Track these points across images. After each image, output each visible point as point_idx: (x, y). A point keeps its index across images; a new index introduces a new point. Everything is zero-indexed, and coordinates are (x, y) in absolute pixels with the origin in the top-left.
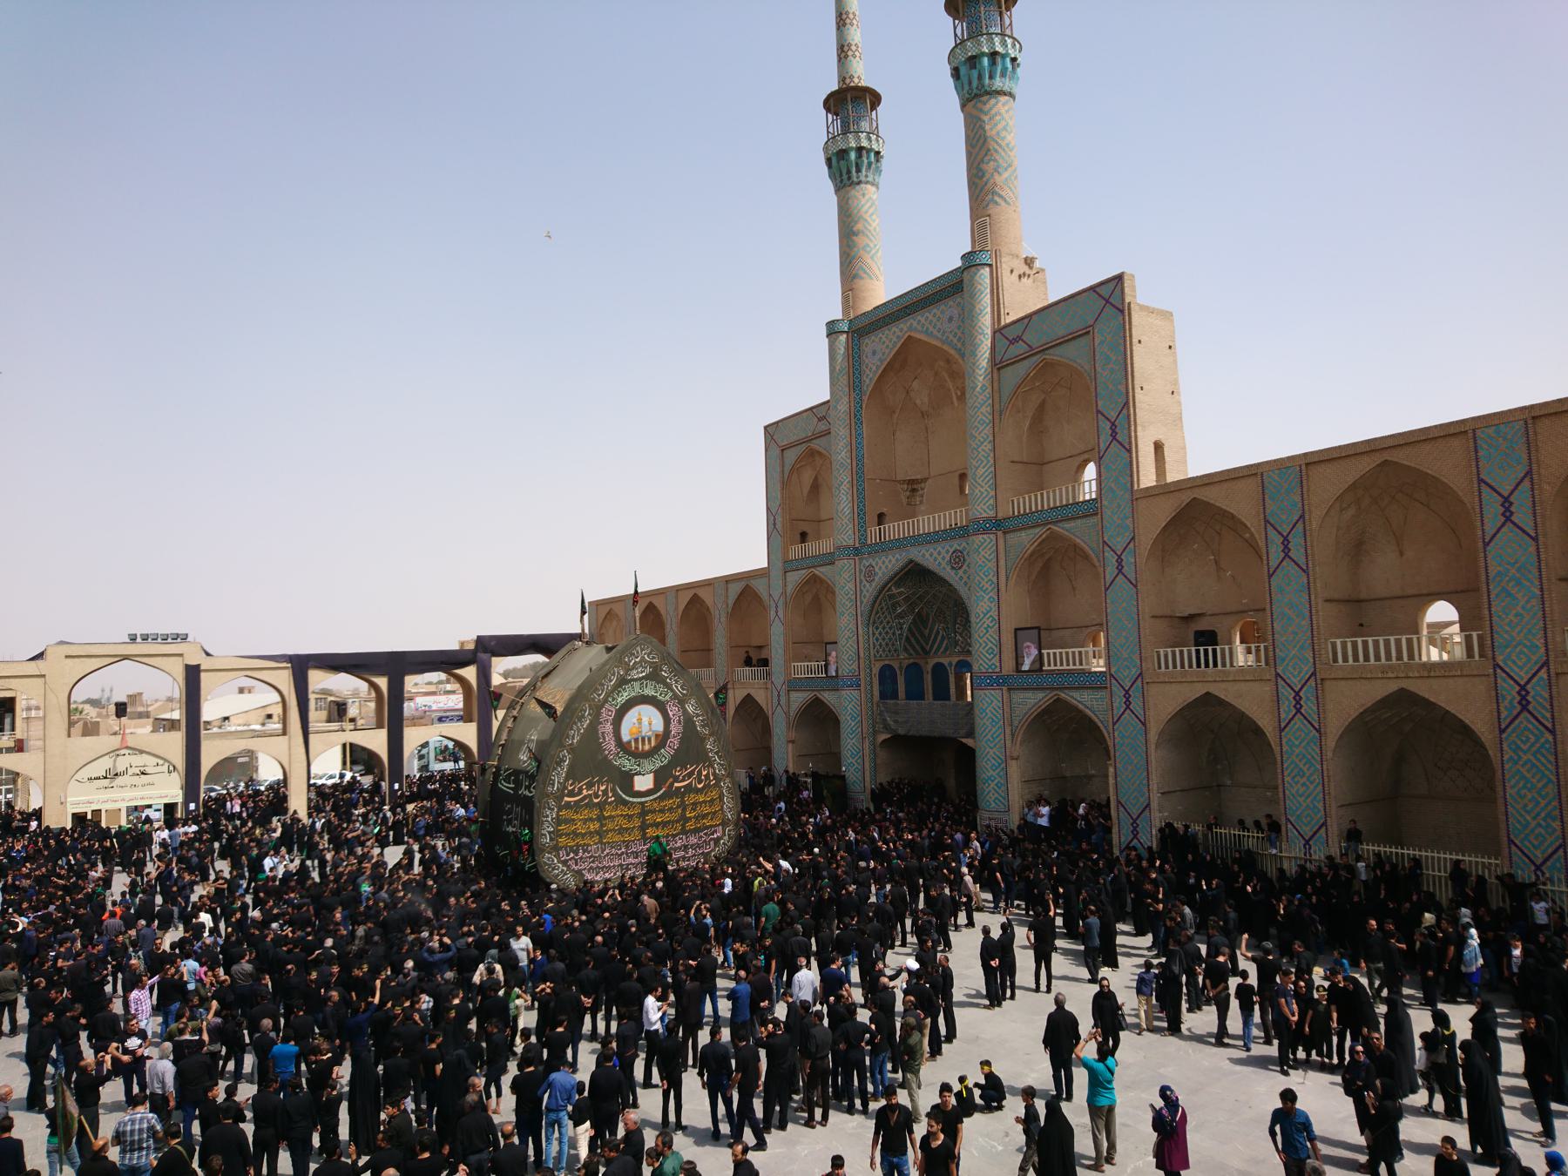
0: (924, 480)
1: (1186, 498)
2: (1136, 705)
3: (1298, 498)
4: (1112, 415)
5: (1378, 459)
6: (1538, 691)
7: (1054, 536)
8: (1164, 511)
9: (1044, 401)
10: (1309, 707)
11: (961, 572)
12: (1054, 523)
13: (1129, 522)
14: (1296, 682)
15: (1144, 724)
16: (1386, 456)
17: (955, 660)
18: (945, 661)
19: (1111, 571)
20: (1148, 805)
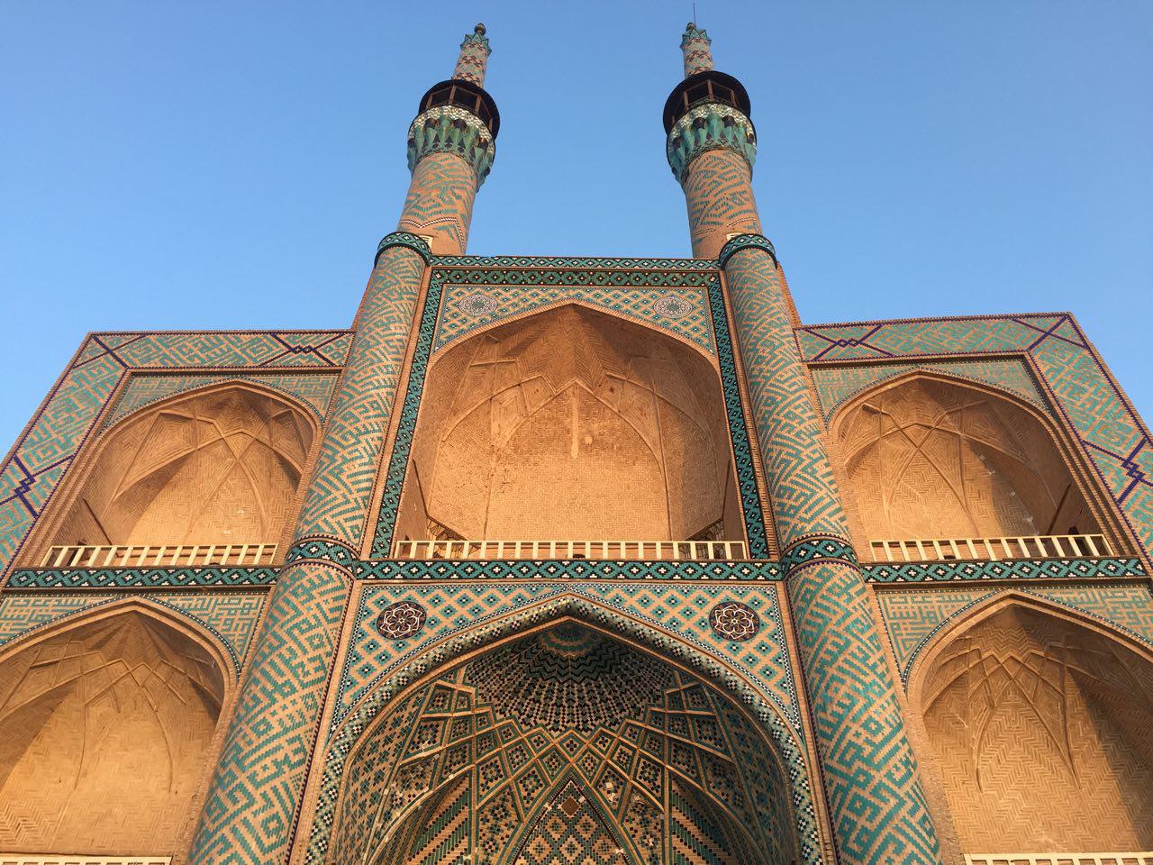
9: (876, 442)
11: (749, 648)
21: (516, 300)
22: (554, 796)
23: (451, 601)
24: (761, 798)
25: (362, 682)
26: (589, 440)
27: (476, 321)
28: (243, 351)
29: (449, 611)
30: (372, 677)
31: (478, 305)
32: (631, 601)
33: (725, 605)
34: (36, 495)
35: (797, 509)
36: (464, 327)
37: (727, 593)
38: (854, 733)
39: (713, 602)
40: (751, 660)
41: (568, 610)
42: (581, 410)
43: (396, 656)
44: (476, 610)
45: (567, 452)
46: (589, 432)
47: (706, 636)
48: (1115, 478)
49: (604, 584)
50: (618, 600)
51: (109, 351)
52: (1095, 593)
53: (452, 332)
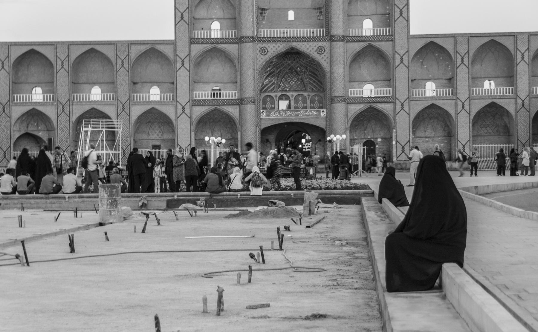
0: (267, 9)
1: (429, 40)
2: (406, 108)
3: (467, 46)
4: (401, 7)
5: (490, 38)
6: (526, 102)
7: (370, 46)
8: (420, 44)
10: (467, 107)
11: (323, 56)
12: (371, 41)
13: (406, 45)
14: (463, 100)
15: (409, 114)
16: (492, 38)
17: (279, 94)
18: (273, 95)
19: (398, 61)
20: (409, 141)
22: (289, 70)
23: (272, 47)
29: (272, 49)
30: (261, 63)
32: (303, 46)
34: (186, 17)
37: (320, 44)
38: (336, 75)
40: (323, 58)
41: (292, 48)
43: (264, 59)
48: (397, 14)
49: (299, 43)
50: (301, 46)
52: (383, 43)
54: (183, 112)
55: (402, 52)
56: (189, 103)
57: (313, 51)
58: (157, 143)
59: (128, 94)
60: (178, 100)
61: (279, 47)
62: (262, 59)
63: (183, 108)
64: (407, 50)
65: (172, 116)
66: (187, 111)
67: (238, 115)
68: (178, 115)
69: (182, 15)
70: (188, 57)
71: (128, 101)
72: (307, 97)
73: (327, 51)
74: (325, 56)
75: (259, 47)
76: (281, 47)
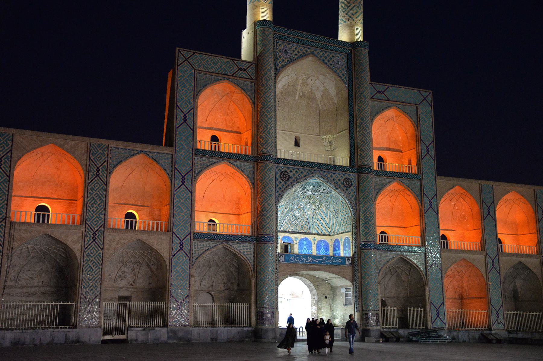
3: (492, 196)
4: (428, 144)
10: (496, 265)
11: (350, 190)
13: (434, 187)
21: (296, 52)
23: (294, 172)
24: (342, 216)
25: (280, 191)
26: (301, 94)
27: (286, 61)
28: (226, 66)
31: (286, 52)
33: (346, 178)
35: (365, 157)
36: (283, 63)
37: (347, 175)
39: (344, 178)
42: (301, 84)
43: (286, 186)
44: (299, 175)
45: (295, 97)
46: (302, 91)
47: (342, 186)
49: (325, 170)
51: (186, 60)
53: (280, 65)
54: (181, 249)
55: (431, 195)
56: (189, 237)
57: (339, 183)
58: (127, 294)
59: (103, 217)
60: (175, 231)
61: (302, 173)
62: (283, 186)
63: (181, 243)
64: (433, 193)
65: (165, 255)
66: (186, 247)
67: (252, 258)
68: (174, 252)
69: (185, 116)
70: (190, 173)
71: (102, 228)
72: (313, 242)
73: (354, 184)
74: (352, 190)
75: (280, 170)
76: (305, 173)
